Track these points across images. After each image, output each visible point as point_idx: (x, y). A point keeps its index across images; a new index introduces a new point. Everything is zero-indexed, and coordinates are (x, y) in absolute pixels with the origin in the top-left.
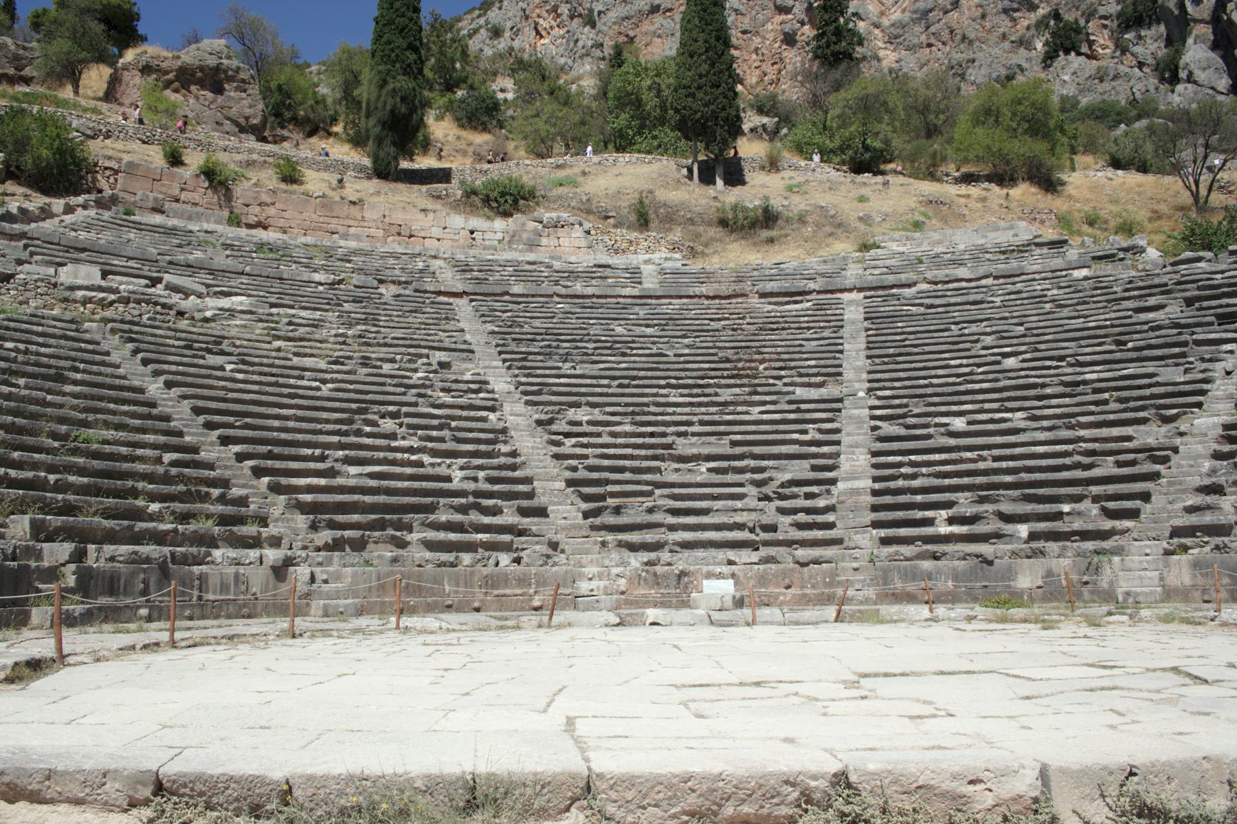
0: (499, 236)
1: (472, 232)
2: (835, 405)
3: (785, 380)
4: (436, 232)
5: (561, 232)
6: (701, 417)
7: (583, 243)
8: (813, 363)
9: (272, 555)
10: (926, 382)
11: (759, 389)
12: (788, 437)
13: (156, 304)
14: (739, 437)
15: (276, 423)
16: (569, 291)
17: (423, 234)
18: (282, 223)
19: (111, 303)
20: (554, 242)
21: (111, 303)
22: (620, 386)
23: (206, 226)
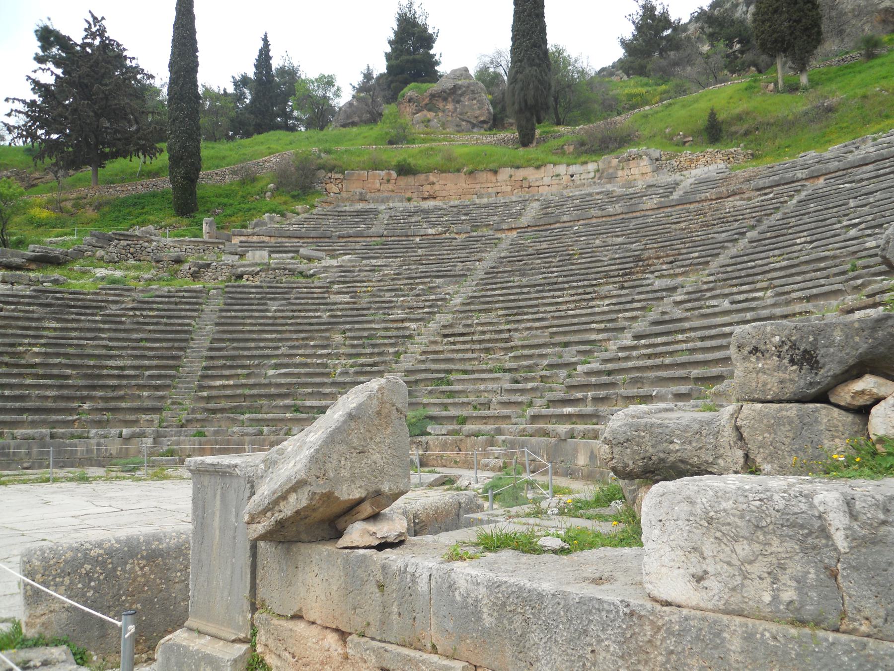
0: (592, 175)
1: (572, 176)
2: (659, 294)
3: (656, 274)
4: (547, 180)
5: (632, 164)
6: (552, 314)
7: (649, 169)
8: (697, 254)
9: (125, 431)
10: (753, 264)
11: (626, 285)
12: (588, 327)
13: (285, 269)
14: (554, 329)
15: (253, 345)
16: (604, 213)
17: (537, 184)
18: (444, 193)
19: (257, 273)
20: (627, 172)
21: (257, 273)
22: (538, 291)
23: (391, 205)
